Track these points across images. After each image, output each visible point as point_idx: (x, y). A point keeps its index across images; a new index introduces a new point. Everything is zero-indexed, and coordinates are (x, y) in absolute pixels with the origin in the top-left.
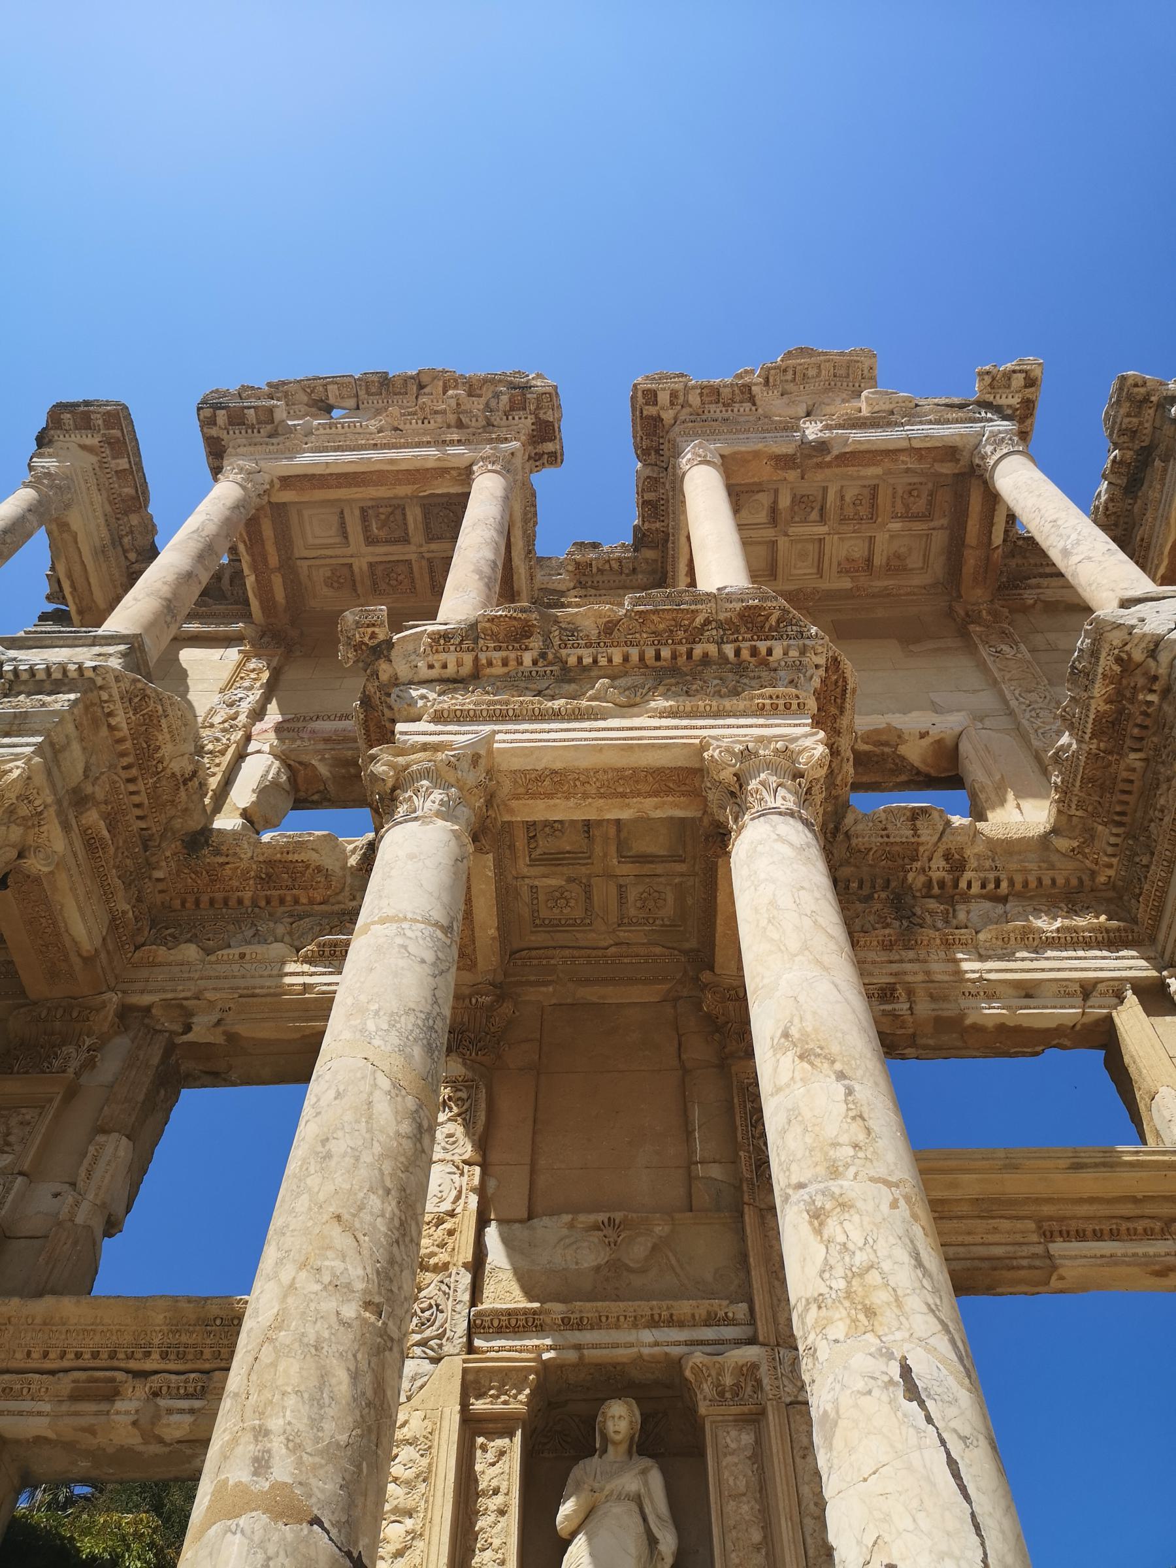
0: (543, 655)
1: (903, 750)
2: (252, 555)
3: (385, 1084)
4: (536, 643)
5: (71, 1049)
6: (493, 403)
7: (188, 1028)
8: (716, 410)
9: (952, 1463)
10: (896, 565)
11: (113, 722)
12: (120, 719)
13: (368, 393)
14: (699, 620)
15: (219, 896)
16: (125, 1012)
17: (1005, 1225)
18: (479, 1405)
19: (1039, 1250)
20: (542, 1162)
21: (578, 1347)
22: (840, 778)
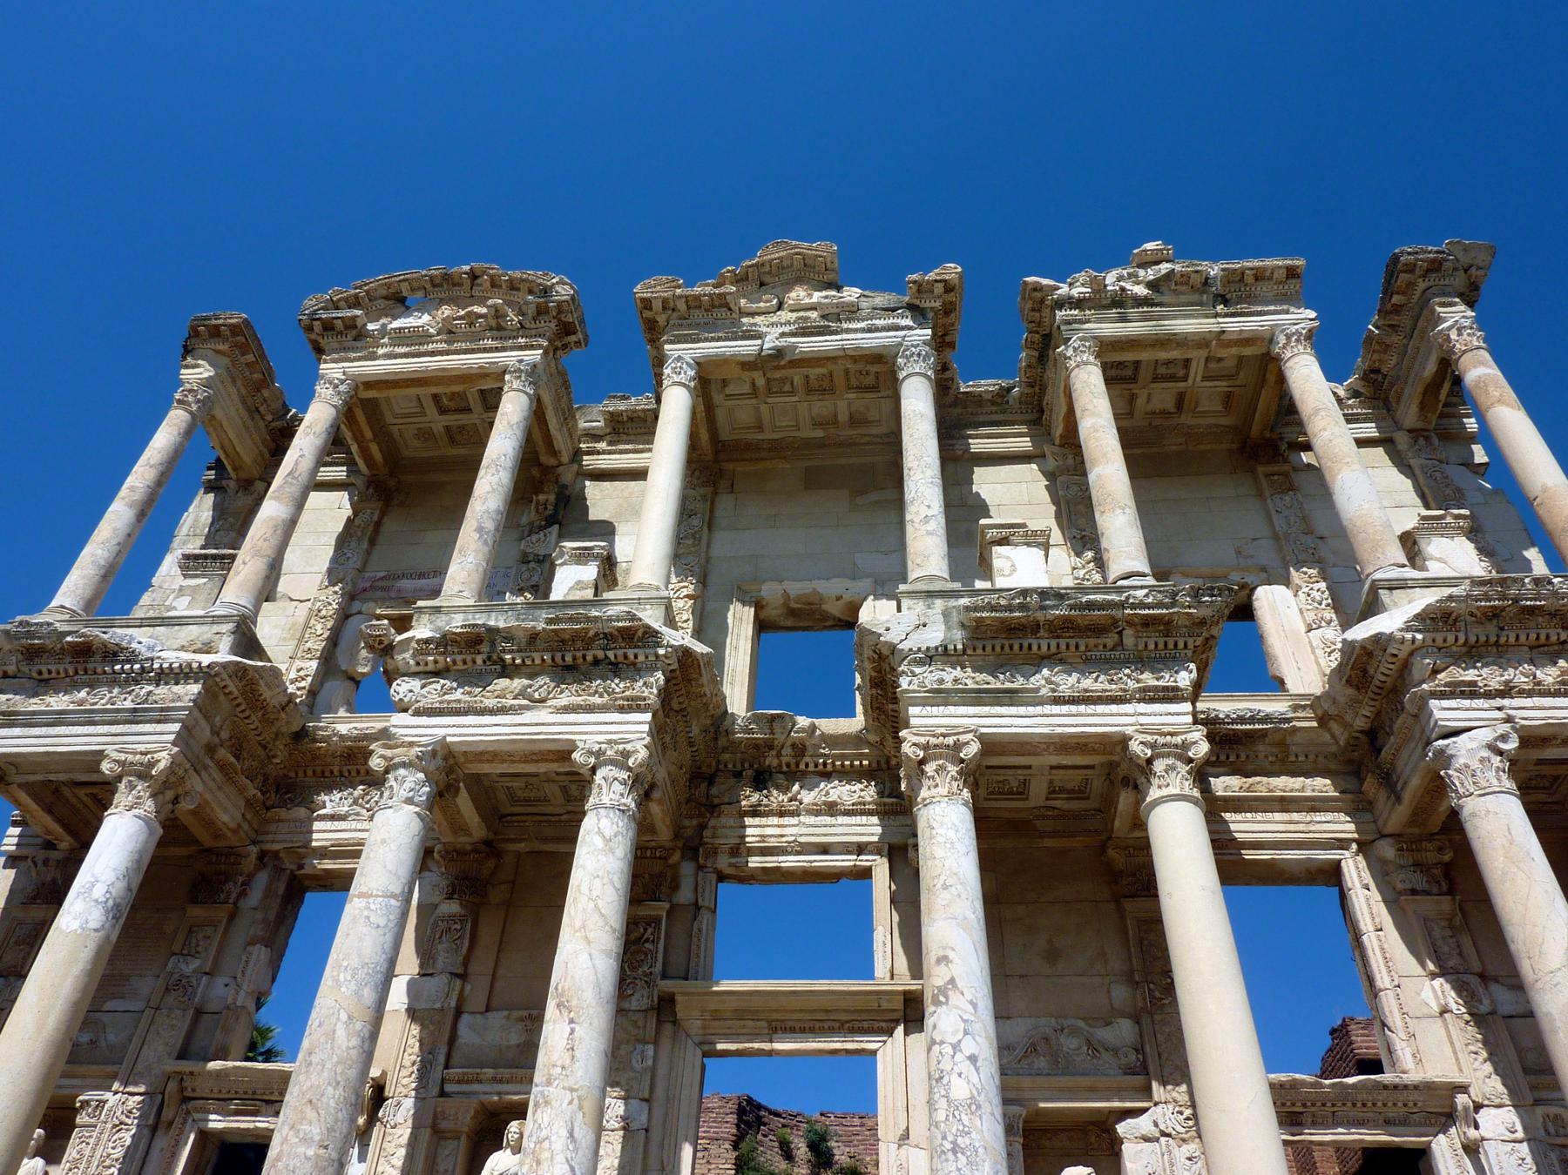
0: (489, 658)
1: (824, 607)
3: (344, 1016)
4: (485, 648)
5: (230, 885)
6: (524, 308)
7: (301, 867)
10: (856, 420)
12: (232, 688)
13: (434, 286)
14: (591, 633)
15: (319, 769)
16: (262, 855)
17: (751, 1023)
18: (443, 1125)
20: (501, 972)
21: (499, 1094)
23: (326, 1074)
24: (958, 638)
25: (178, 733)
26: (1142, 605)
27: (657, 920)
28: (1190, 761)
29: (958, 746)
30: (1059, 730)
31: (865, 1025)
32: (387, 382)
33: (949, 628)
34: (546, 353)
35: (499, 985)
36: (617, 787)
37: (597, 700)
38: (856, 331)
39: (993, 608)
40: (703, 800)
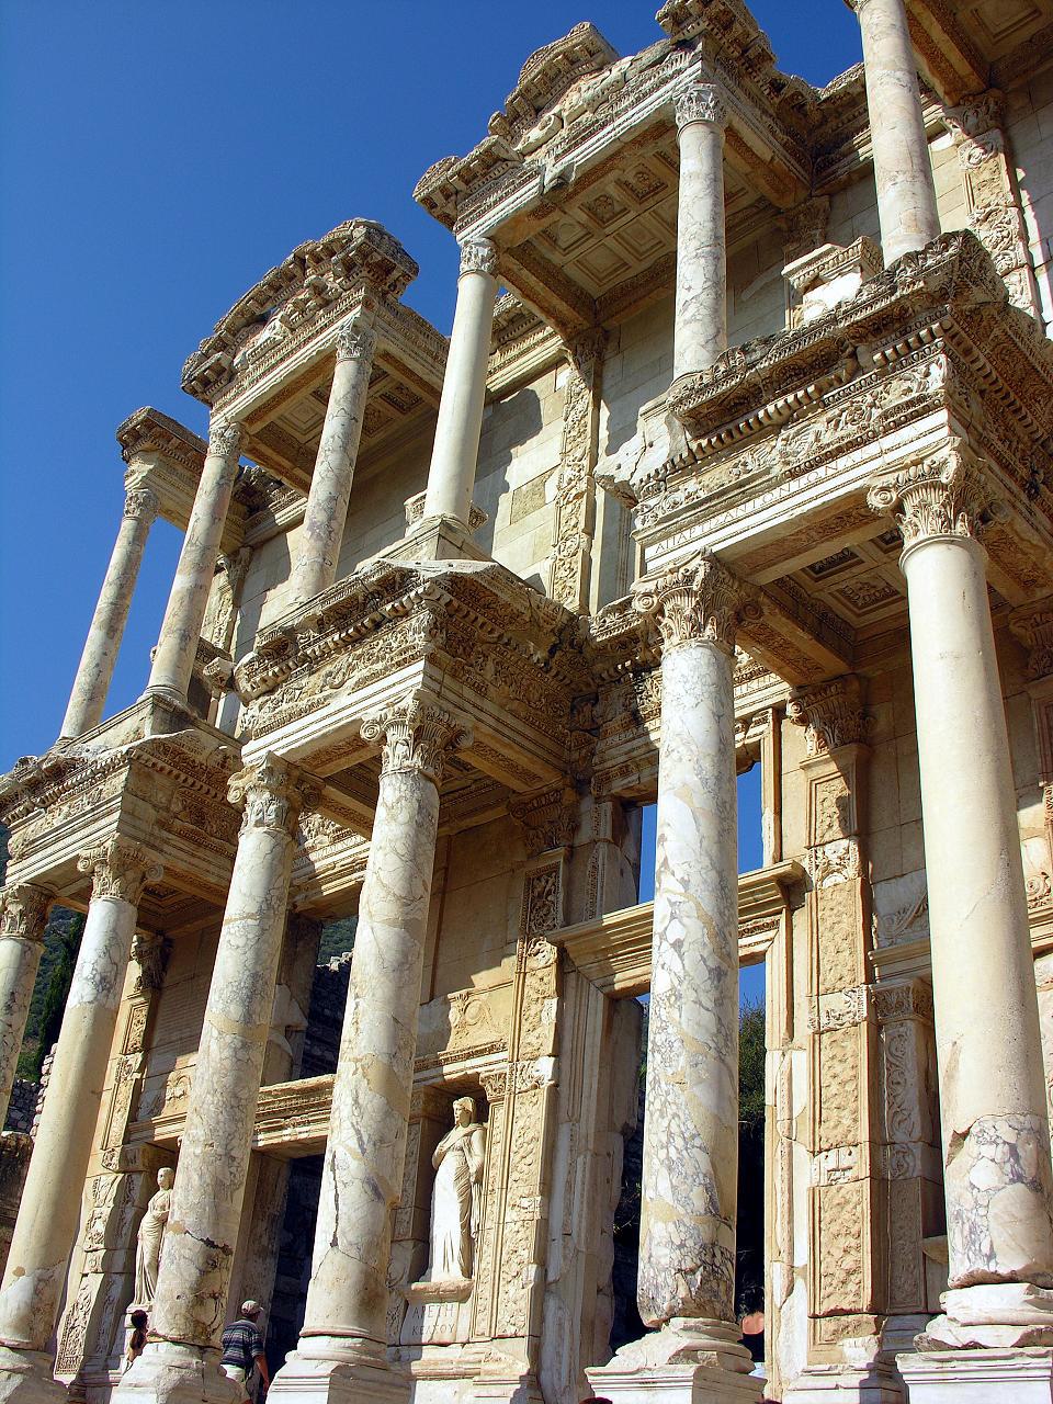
2: (272, 467)
4: (290, 650)
9: (337, 1195)
12: (160, 764)
14: (361, 598)
20: (441, 960)
22: (541, 621)
23: (205, 1084)
24: (685, 442)
26: (856, 308)
27: (555, 868)
28: (944, 487)
29: (689, 579)
30: (798, 511)
31: (750, 925)
33: (674, 437)
34: (367, 304)
35: (440, 972)
36: (401, 750)
37: (380, 666)
38: (626, 110)
39: (701, 391)
40: (587, 725)
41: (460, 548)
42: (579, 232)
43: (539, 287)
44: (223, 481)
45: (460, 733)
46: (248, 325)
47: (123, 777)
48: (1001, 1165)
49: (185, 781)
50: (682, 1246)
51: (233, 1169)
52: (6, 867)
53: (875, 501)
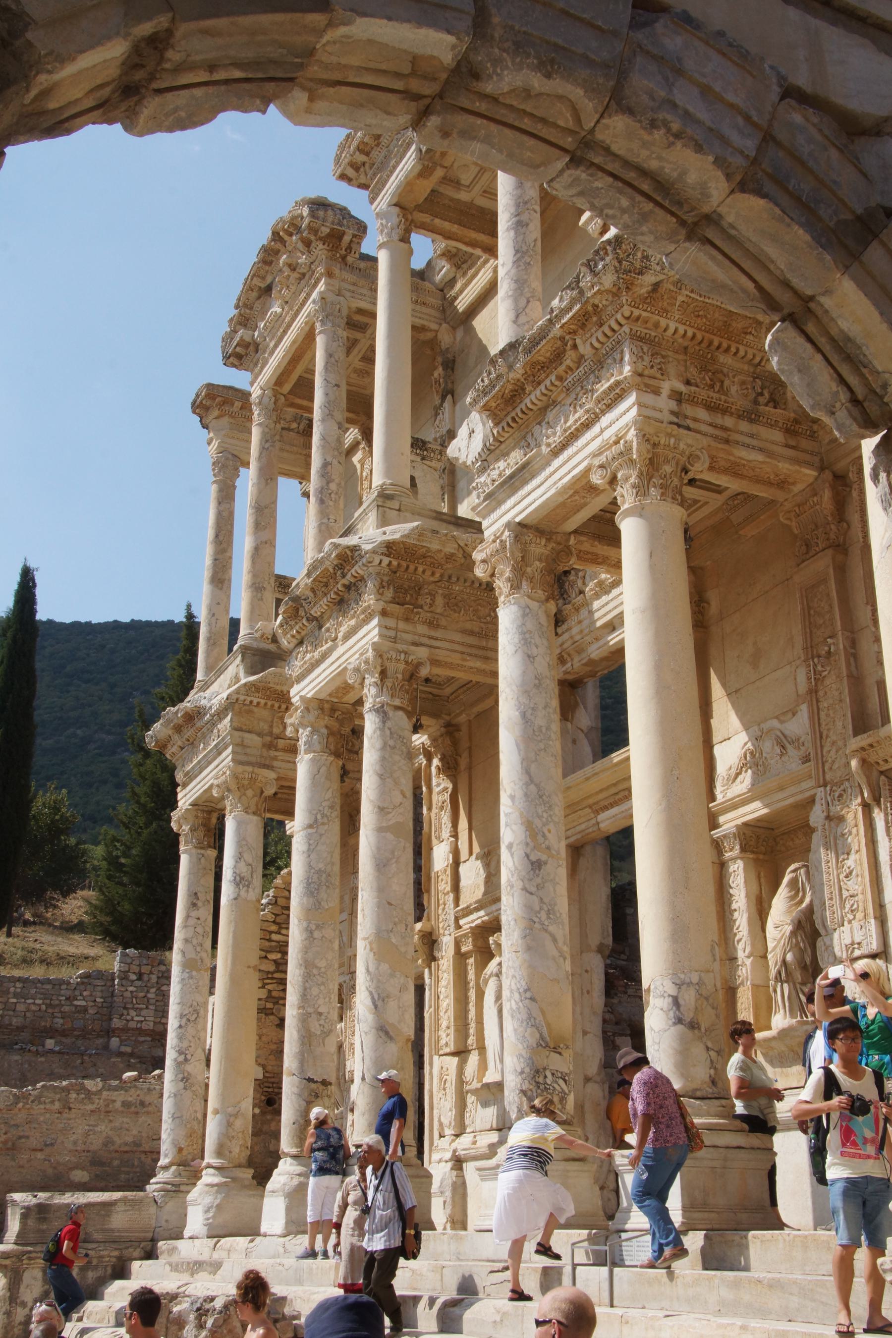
4: (302, 613)
8: (377, 155)
11: (255, 703)
12: (255, 701)
14: (331, 570)
19: (594, 821)
25: (233, 752)
26: (564, 311)
30: (560, 485)
32: (282, 374)
34: (329, 274)
41: (399, 510)
42: (474, 170)
43: (455, 228)
44: (267, 445)
45: (419, 664)
46: (259, 298)
47: (229, 718)
48: (667, 1013)
49: (279, 707)
50: (522, 1073)
51: (322, 1022)
52: (176, 794)
53: (596, 479)
